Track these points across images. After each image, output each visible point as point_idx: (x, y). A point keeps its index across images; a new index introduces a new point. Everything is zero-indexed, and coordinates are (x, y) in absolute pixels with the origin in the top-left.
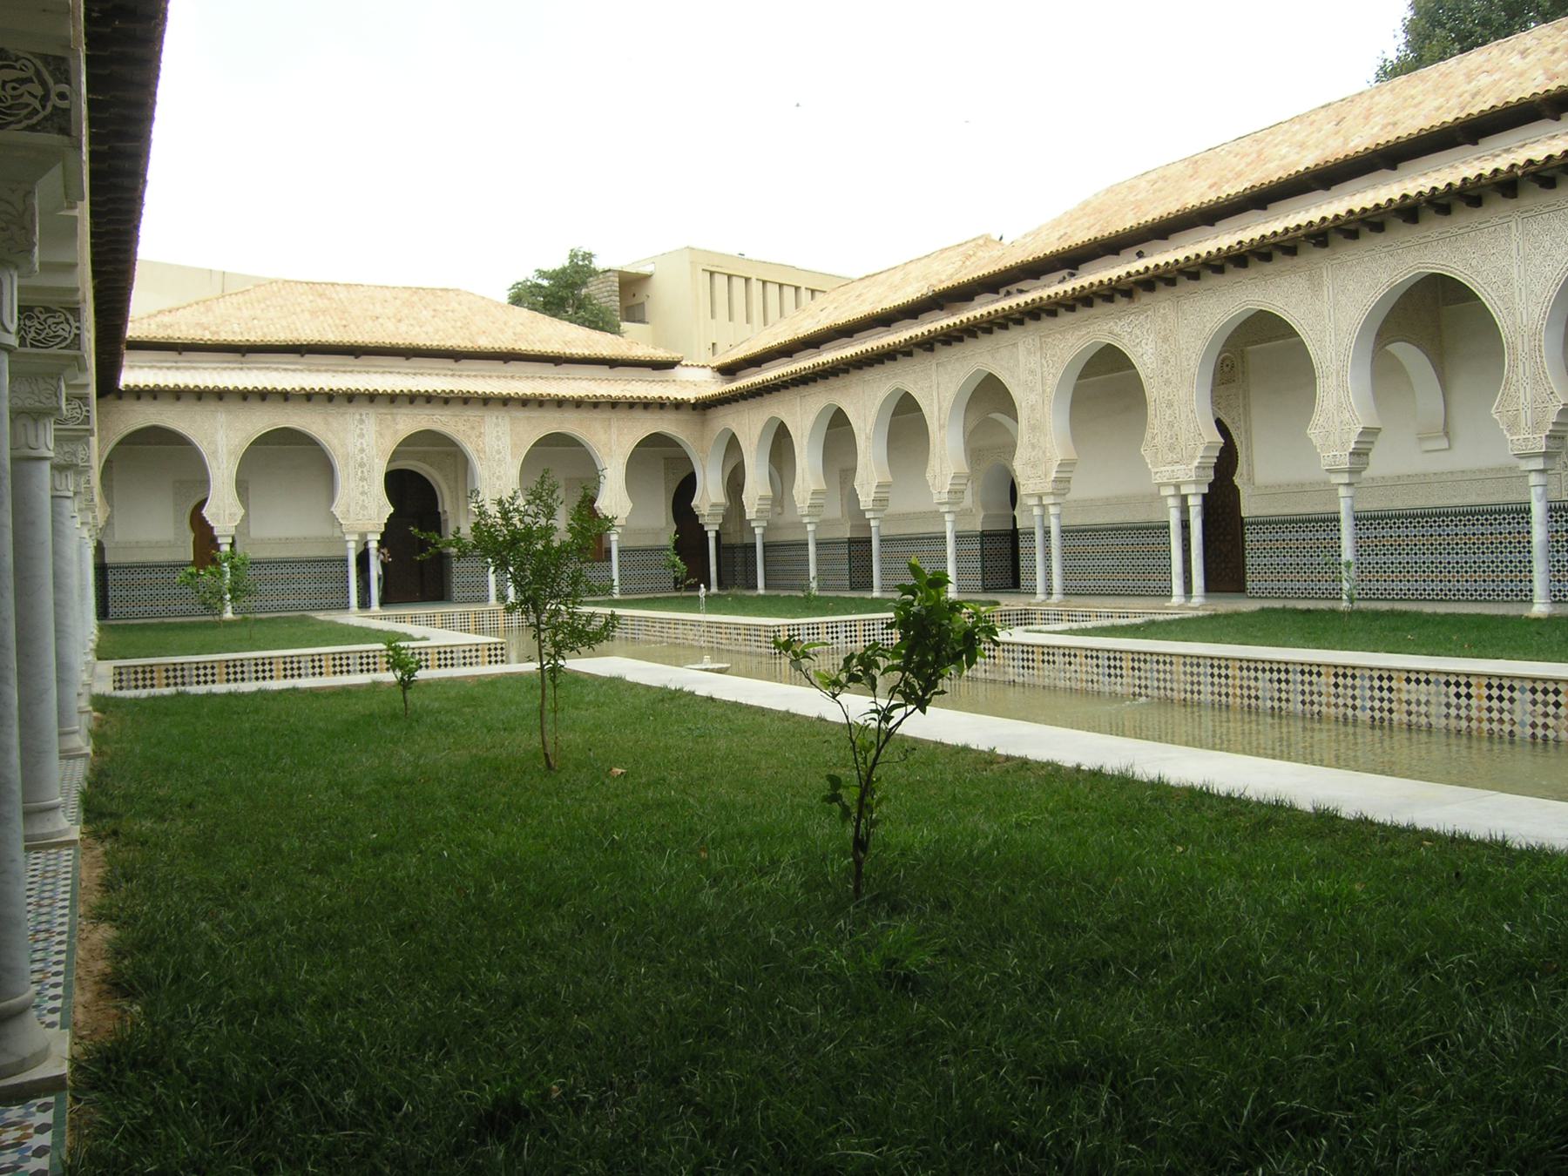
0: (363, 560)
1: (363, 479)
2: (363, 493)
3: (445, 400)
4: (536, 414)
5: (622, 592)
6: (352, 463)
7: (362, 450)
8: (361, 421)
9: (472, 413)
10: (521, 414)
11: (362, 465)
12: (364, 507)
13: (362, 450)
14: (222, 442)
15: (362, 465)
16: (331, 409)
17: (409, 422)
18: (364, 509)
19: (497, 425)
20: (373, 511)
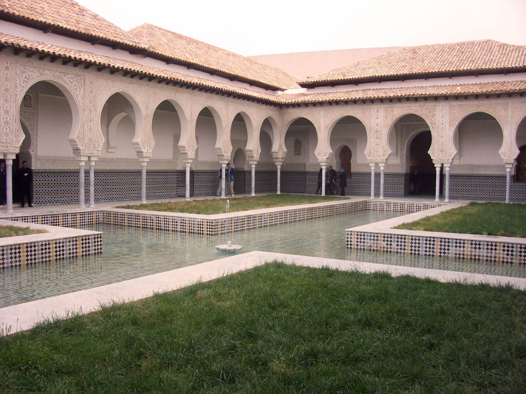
0: (377, 175)
1: (377, 138)
2: (377, 145)
3: (416, 99)
4: (464, 103)
5: (510, 199)
6: (372, 131)
7: (377, 125)
8: (378, 111)
9: (430, 105)
10: (455, 103)
11: (377, 132)
12: (377, 151)
13: (377, 125)
14: (323, 122)
15: (377, 132)
16: (365, 106)
17: (400, 110)
18: (378, 153)
19: (442, 110)
20: (381, 152)
